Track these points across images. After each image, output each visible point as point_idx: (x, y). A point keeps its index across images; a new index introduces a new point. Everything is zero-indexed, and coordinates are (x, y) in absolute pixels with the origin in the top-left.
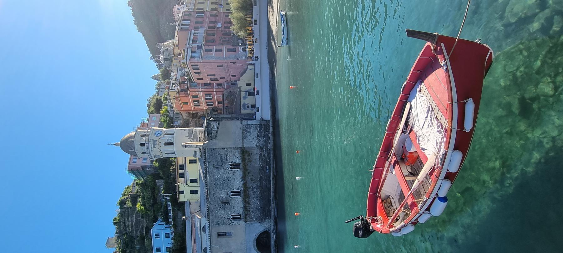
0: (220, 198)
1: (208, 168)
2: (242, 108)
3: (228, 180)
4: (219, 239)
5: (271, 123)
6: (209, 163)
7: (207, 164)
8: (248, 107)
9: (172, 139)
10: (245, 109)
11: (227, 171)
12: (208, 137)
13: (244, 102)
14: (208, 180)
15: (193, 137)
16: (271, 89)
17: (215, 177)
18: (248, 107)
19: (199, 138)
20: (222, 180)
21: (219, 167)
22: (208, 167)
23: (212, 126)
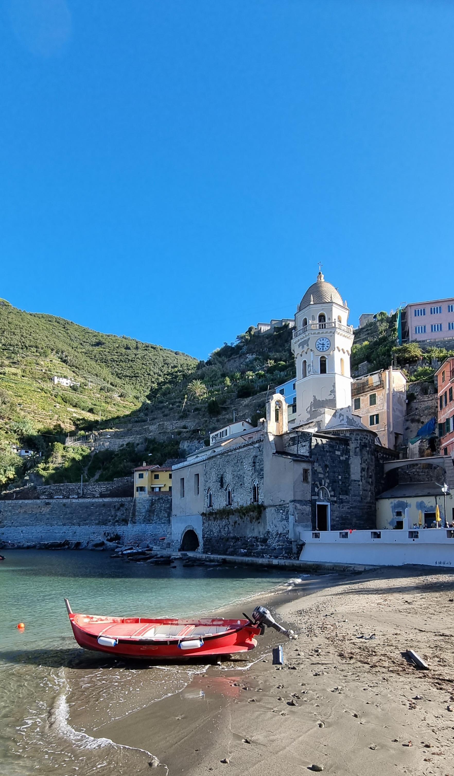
0: (225, 474)
1: (252, 447)
2: (397, 500)
3: (241, 483)
4: (194, 476)
5: (296, 562)
6: (258, 448)
7: (257, 445)
8: (397, 515)
9: (311, 373)
10: (394, 507)
11: (250, 481)
12: (290, 440)
13: (410, 506)
14: (241, 450)
15: (313, 410)
16: (335, 566)
17: (244, 461)
18: (397, 515)
19: (312, 422)
20: (241, 473)
21: (254, 466)
22: (254, 447)
23: (304, 444)
